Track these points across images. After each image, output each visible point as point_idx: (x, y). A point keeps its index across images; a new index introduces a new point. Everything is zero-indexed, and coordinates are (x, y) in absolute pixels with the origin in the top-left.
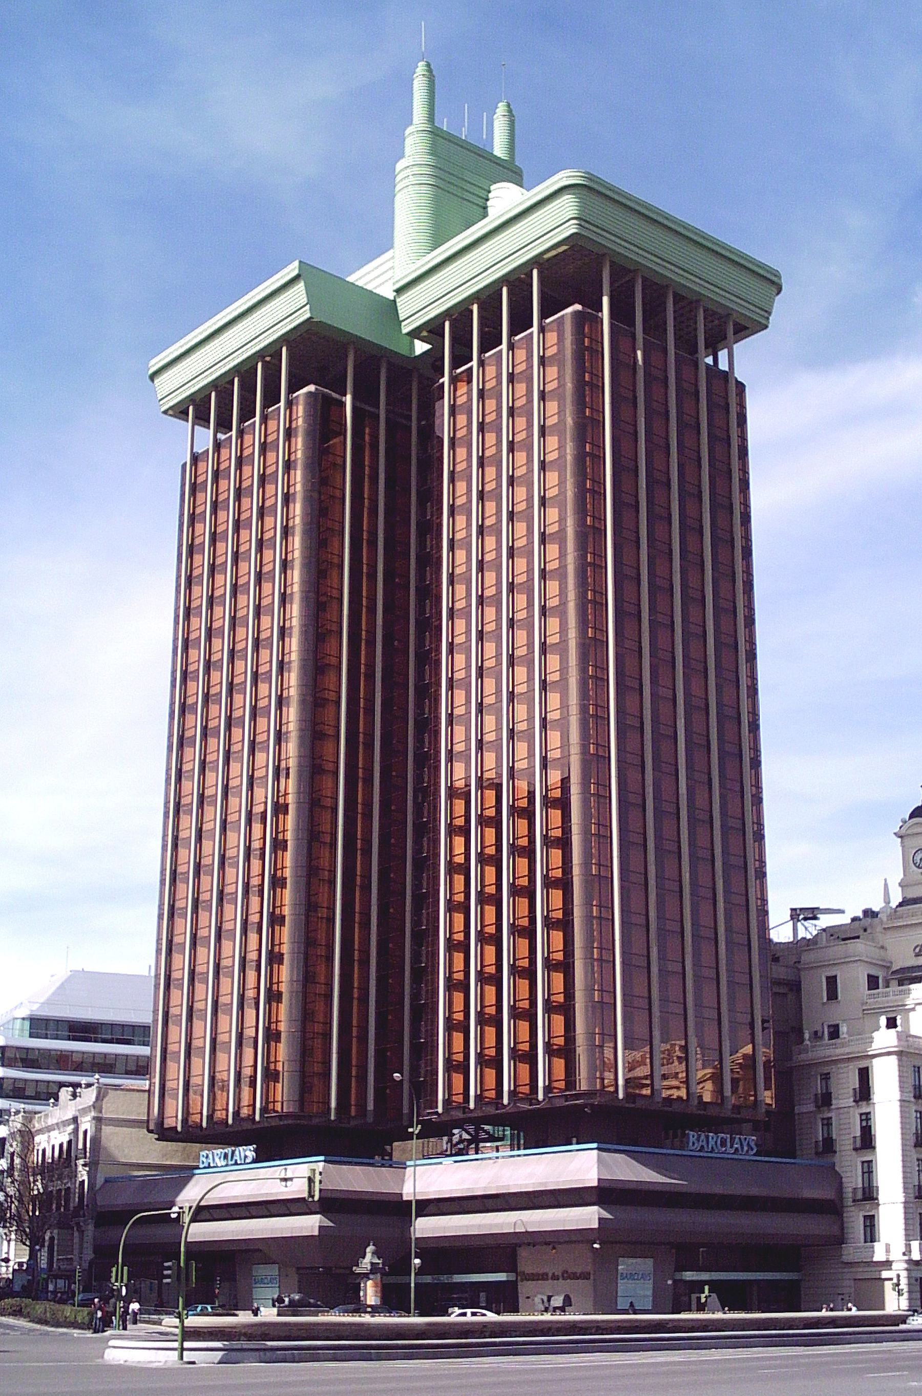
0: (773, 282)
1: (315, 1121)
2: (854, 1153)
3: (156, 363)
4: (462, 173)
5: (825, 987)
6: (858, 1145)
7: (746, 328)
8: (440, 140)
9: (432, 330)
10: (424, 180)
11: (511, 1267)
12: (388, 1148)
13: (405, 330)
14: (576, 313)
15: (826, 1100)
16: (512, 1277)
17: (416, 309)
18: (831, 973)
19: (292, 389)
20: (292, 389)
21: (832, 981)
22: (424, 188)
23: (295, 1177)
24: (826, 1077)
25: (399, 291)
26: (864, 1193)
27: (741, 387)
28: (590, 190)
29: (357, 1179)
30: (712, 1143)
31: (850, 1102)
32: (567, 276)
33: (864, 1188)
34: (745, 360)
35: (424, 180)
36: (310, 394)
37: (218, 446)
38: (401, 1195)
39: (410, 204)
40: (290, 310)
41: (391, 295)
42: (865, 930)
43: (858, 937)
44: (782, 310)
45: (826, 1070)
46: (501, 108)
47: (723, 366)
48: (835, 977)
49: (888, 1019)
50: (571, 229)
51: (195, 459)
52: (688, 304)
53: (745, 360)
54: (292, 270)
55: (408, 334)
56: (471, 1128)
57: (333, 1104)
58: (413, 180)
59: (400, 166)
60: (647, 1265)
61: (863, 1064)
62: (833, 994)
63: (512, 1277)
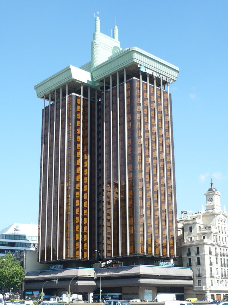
2: (196, 266)
5: (189, 229)
6: (197, 264)
11: (121, 292)
12: (91, 265)
13: (94, 81)
15: (189, 254)
16: (121, 294)
18: (191, 226)
24: (189, 250)
26: (198, 275)
30: (165, 264)
31: (195, 255)
33: (198, 274)
38: (140, 273)
42: (198, 216)
43: (196, 218)
45: (189, 248)
48: (191, 227)
49: (203, 236)
56: (111, 261)
60: (151, 291)
61: (198, 246)
62: (191, 231)
63: (121, 294)
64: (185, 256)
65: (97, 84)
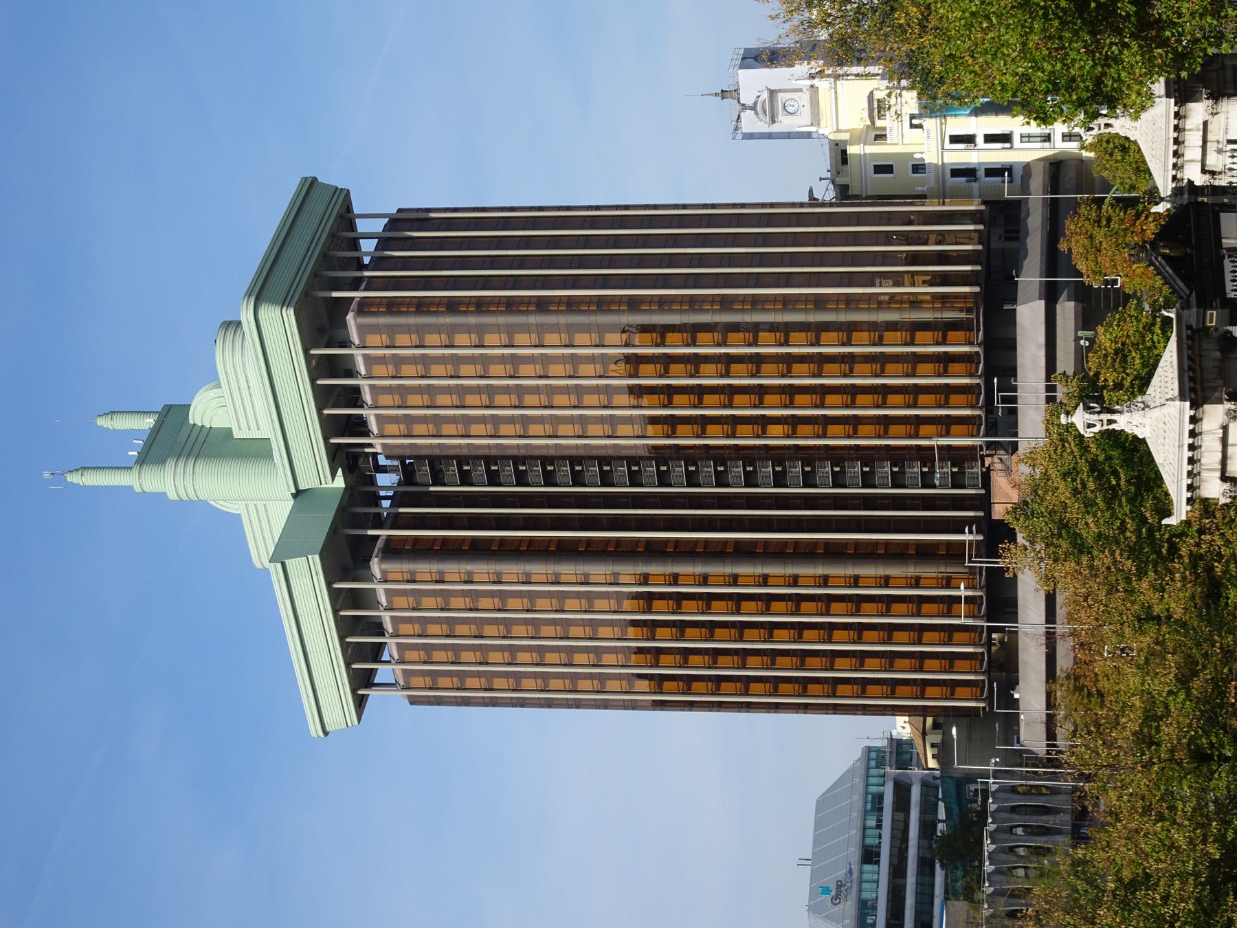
3: (315, 730)
21: (879, 169)
22: (197, 470)
27: (400, 211)
28: (261, 293)
44: (331, 177)
46: (104, 422)
47: (378, 226)
58: (189, 478)
62: (888, 169)
65: (340, 482)
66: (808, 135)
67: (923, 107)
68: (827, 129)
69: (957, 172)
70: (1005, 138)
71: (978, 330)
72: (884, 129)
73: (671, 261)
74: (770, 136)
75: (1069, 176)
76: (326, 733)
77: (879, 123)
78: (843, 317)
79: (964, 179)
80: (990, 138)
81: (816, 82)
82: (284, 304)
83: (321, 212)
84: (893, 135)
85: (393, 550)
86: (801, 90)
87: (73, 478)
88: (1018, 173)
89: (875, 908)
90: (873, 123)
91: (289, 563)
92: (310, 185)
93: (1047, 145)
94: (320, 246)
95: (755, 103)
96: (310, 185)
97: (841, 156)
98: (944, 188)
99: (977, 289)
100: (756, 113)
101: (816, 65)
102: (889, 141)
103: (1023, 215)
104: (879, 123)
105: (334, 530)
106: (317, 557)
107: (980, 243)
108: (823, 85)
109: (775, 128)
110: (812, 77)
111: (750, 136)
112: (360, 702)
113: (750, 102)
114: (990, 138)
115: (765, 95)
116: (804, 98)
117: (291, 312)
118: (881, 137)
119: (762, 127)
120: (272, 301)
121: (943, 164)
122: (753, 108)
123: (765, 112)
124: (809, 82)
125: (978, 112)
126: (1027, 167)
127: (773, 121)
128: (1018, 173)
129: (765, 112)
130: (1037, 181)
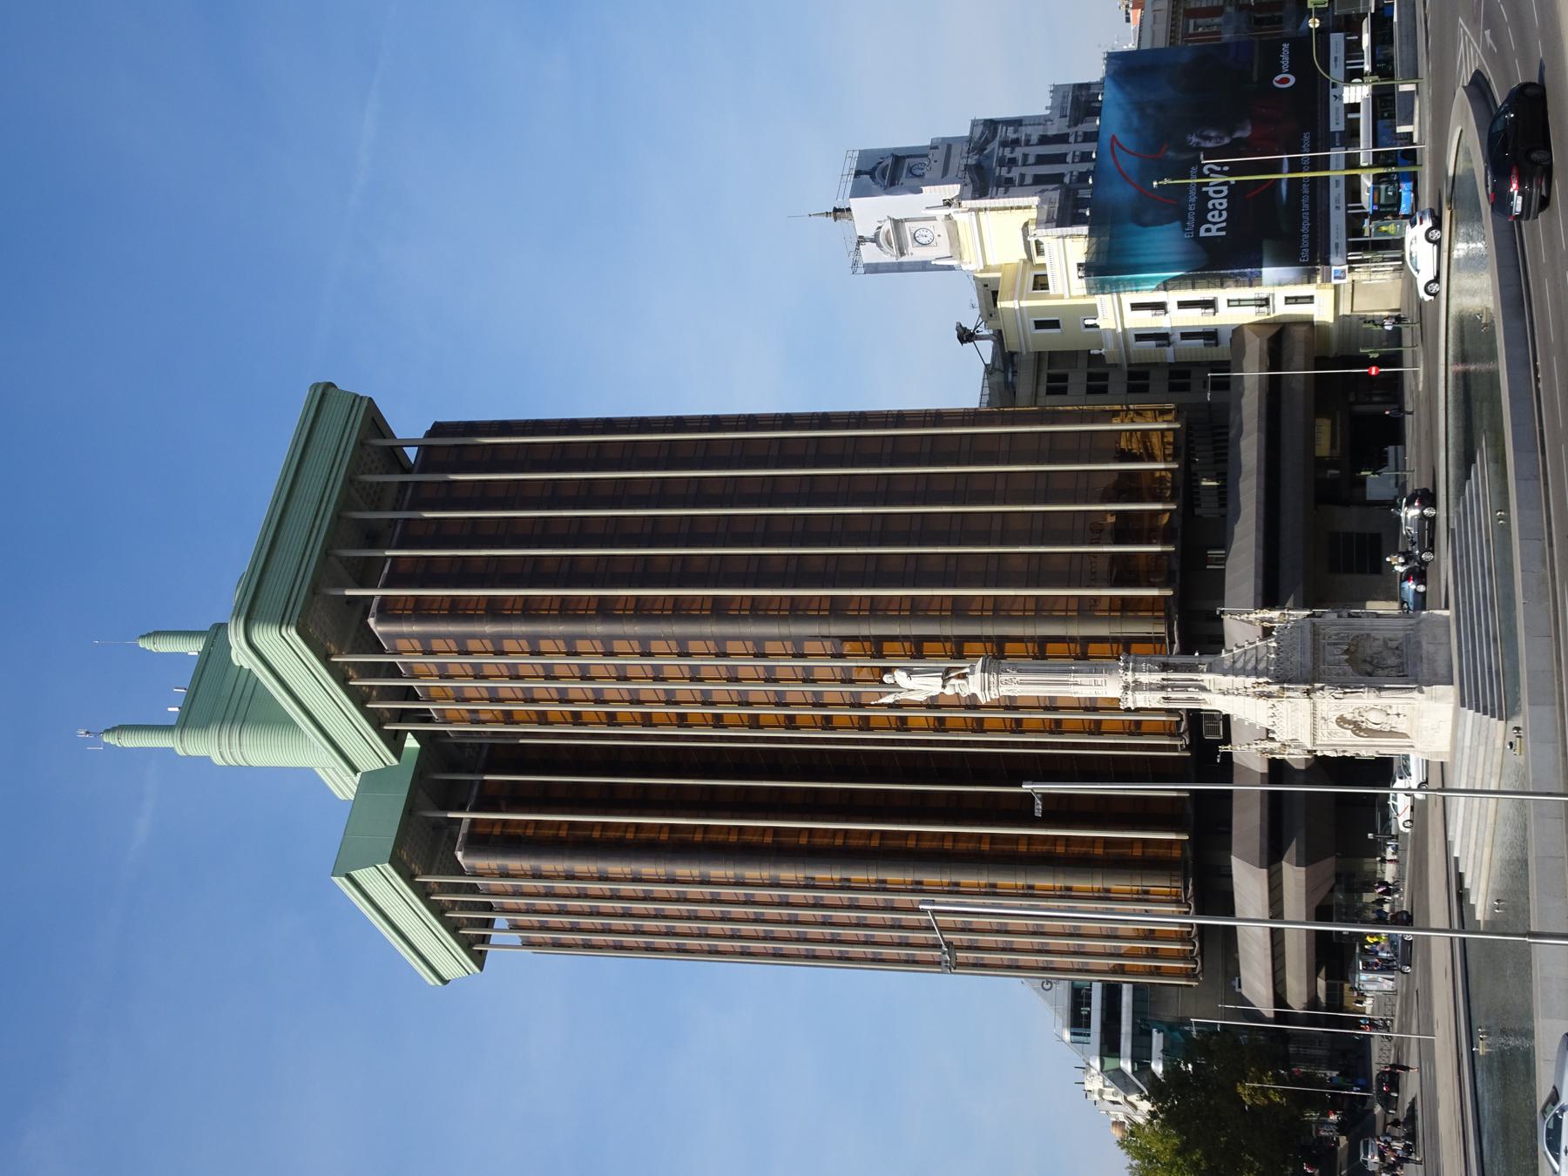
0: (323, 394)
1: (1189, 853)
4: (222, 698)
7: (375, 423)
8: (188, 721)
9: (394, 742)
10: (235, 740)
13: (395, 762)
14: (379, 621)
15: (1162, 337)
17: (370, 753)
19: (460, 871)
20: (460, 871)
21: (1040, 325)
23: (1248, 883)
25: (355, 770)
27: (438, 429)
28: (251, 614)
29: (1247, 823)
32: (337, 633)
34: (409, 425)
35: (235, 740)
36: (465, 856)
37: (515, 927)
39: (257, 751)
40: (384, 885)
41: (357, 778)
50: (292, 633)
51: (528, 944)
52: (354, 493)
53: (409, 425)
54: (341, 882)
55: (398, 759)
57: (1172, 836)
59: (217, 760)
62: (1054, 324)
64: (1169, 354)
65: (411, 743)
66: (951, 268)
67: (1089, 288)
68: (972, 263)
69: (1140, 337)
70: (1209, 304)
71: (1172, 642)
72: (1044, 266)
73: (768, 532)
74: (899, 268)
75: (1297, 346)
76: (444, 981)
77: (1038, 260)
78: (989, 630)
79: (1153, 343)
80: (1183, 305)
81: (950, 211)
82: (282, 621)
83: (333, 447)
84: (1056, 283)
85: (481, 840)
86: (934, 219)
87: (109, 739)
88: (1225, 338)
89: (1089, 997)
90: (1030, 258)
91: (355, 874)
92: (324, 393)
93: (1264, 309)
94: (331, 507)
95: (877, 235)
96: (324, 393)
97: (990, 293)
98: (1127, 352)
99: (1169, 593)
100: (879, 246)
101: (953, 190)
102: (1051, 291)
103: (1232, 433)
104: (1038, 260)
105: (410, 810)
106: (387, 865)
107: (1175, 457)
108: (963, 219)
109: (904, 259)
110: (948, 204)
111: (873, 269)
112: (479, 959)
113: (870, 234)
114: (1183, 305)
115: (888, 226)
116: (940, 228)
117: (293, 631)
118: (1041, 283)
119: (888, 257)
120: (267, 620)
121: (1124, 330)
122: (875, 240)
123: (890, 244)
124: (947, 211)
125: (1165, 286)
126: (1238, 331)
127: (902, 254)
128: (1225, 338)
129: (890, 244)
130: (1255, 348)
